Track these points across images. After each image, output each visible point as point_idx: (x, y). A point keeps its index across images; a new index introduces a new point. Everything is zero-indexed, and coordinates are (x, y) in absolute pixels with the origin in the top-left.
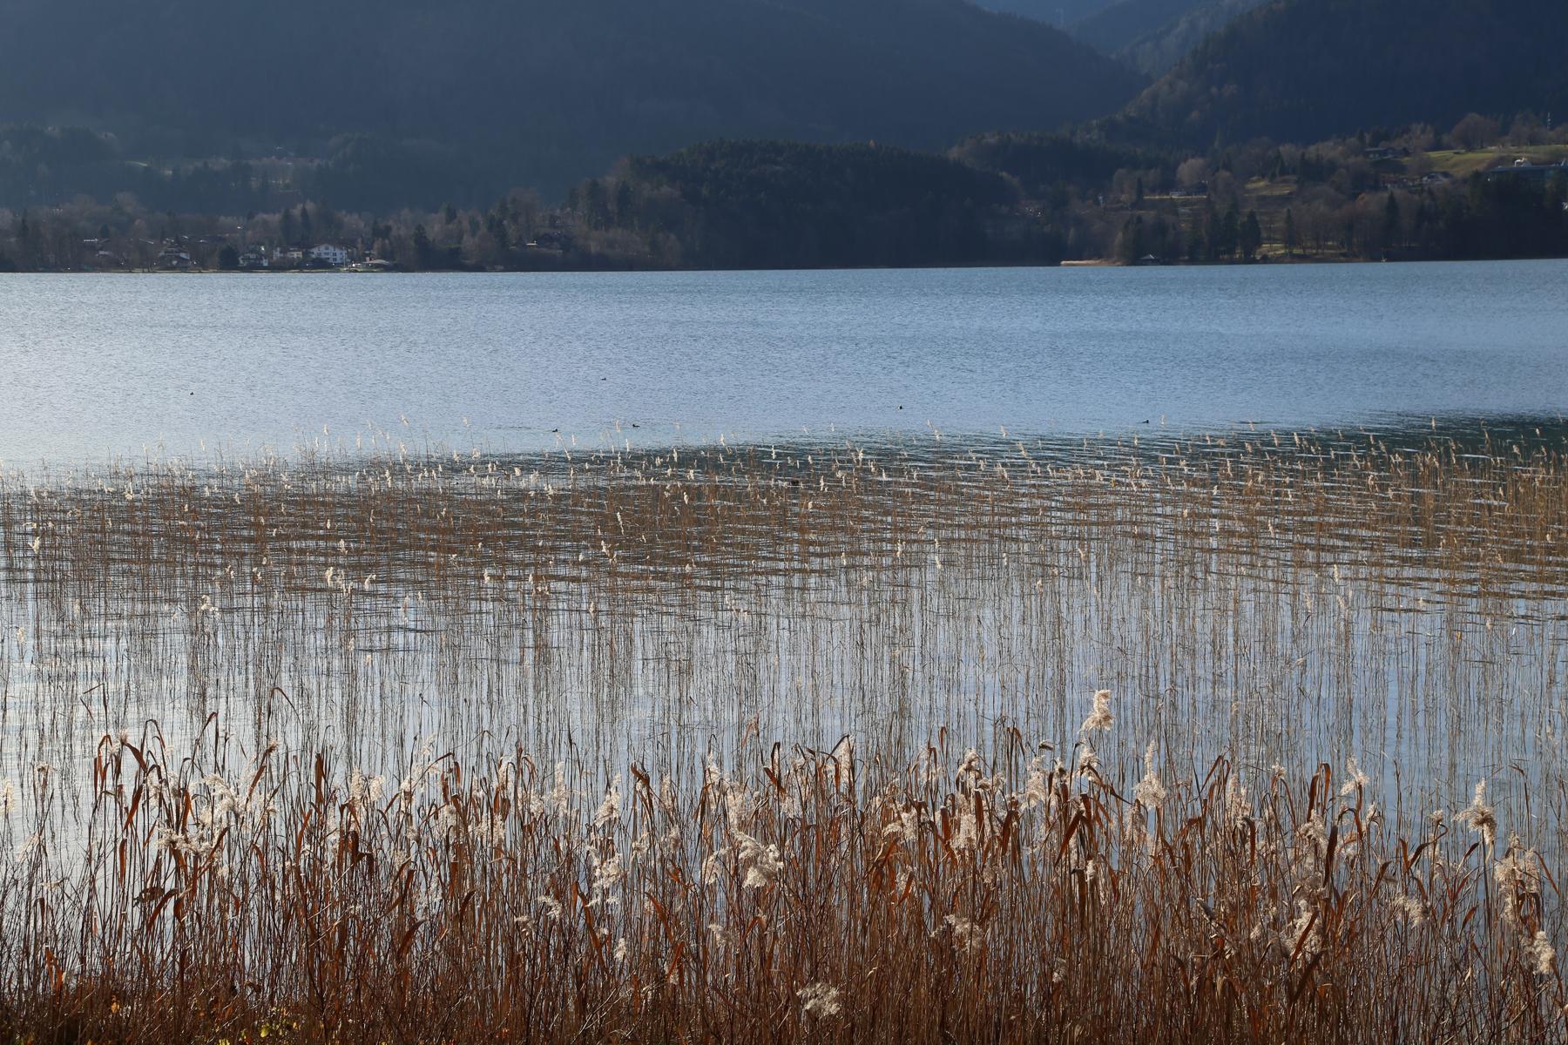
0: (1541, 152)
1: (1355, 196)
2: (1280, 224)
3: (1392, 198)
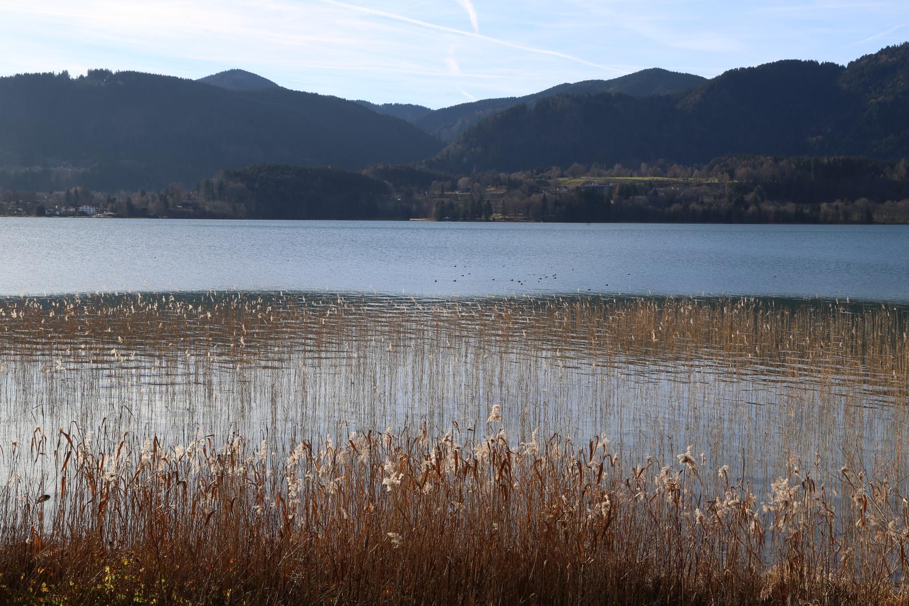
0: (602, 179)
1: (530, 195)
2: (500, 206)
3: (544, 196)
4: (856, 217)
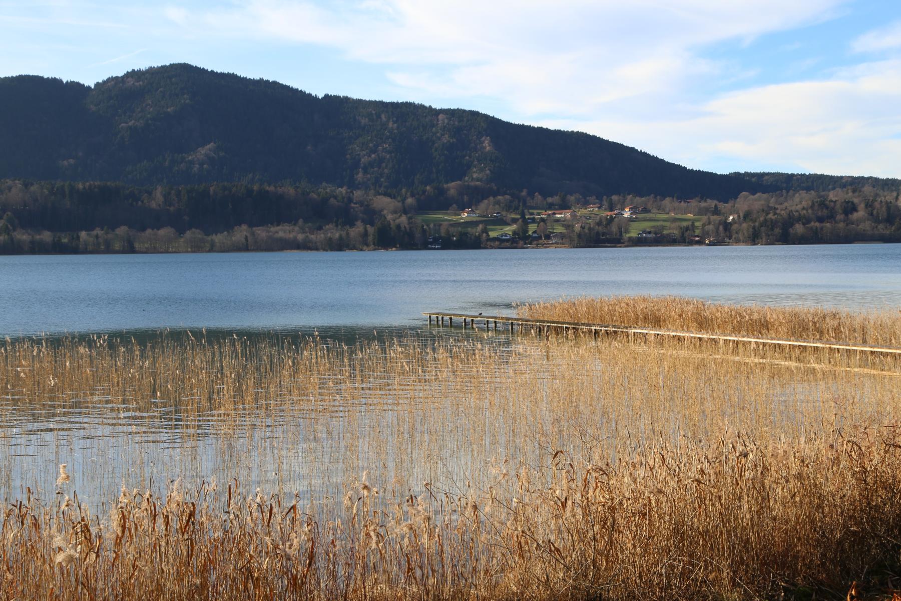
4: (117, 246)
